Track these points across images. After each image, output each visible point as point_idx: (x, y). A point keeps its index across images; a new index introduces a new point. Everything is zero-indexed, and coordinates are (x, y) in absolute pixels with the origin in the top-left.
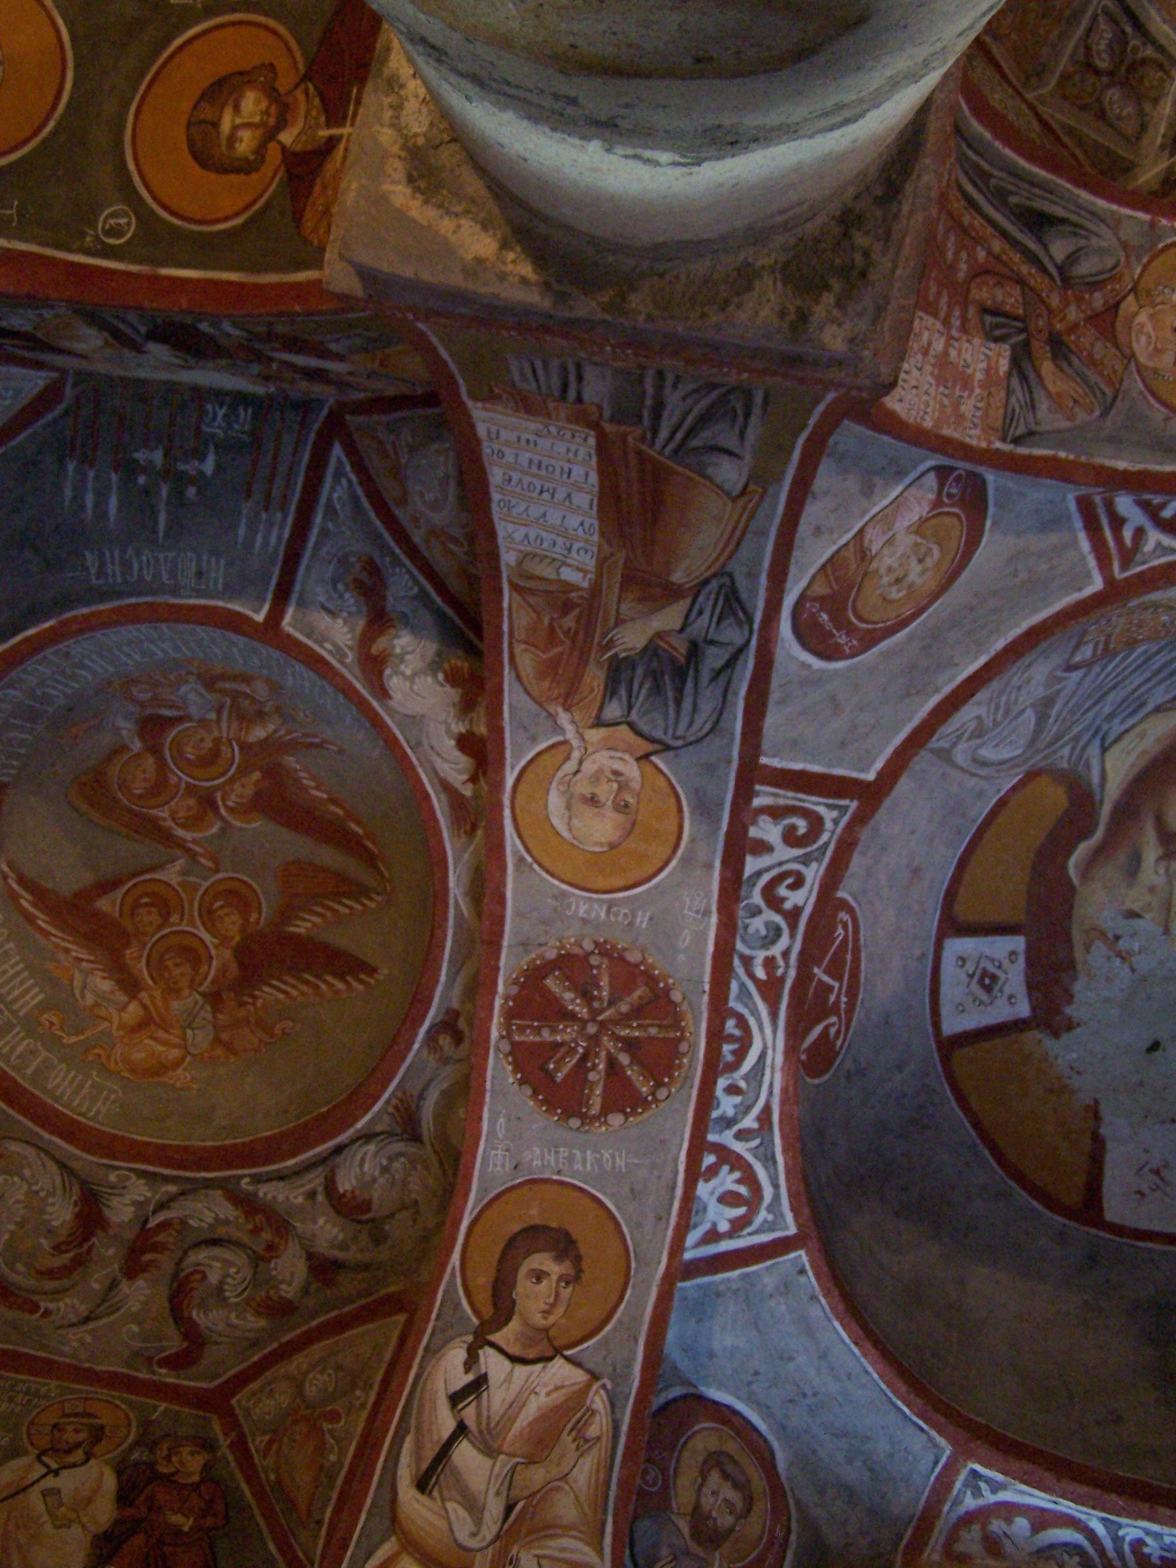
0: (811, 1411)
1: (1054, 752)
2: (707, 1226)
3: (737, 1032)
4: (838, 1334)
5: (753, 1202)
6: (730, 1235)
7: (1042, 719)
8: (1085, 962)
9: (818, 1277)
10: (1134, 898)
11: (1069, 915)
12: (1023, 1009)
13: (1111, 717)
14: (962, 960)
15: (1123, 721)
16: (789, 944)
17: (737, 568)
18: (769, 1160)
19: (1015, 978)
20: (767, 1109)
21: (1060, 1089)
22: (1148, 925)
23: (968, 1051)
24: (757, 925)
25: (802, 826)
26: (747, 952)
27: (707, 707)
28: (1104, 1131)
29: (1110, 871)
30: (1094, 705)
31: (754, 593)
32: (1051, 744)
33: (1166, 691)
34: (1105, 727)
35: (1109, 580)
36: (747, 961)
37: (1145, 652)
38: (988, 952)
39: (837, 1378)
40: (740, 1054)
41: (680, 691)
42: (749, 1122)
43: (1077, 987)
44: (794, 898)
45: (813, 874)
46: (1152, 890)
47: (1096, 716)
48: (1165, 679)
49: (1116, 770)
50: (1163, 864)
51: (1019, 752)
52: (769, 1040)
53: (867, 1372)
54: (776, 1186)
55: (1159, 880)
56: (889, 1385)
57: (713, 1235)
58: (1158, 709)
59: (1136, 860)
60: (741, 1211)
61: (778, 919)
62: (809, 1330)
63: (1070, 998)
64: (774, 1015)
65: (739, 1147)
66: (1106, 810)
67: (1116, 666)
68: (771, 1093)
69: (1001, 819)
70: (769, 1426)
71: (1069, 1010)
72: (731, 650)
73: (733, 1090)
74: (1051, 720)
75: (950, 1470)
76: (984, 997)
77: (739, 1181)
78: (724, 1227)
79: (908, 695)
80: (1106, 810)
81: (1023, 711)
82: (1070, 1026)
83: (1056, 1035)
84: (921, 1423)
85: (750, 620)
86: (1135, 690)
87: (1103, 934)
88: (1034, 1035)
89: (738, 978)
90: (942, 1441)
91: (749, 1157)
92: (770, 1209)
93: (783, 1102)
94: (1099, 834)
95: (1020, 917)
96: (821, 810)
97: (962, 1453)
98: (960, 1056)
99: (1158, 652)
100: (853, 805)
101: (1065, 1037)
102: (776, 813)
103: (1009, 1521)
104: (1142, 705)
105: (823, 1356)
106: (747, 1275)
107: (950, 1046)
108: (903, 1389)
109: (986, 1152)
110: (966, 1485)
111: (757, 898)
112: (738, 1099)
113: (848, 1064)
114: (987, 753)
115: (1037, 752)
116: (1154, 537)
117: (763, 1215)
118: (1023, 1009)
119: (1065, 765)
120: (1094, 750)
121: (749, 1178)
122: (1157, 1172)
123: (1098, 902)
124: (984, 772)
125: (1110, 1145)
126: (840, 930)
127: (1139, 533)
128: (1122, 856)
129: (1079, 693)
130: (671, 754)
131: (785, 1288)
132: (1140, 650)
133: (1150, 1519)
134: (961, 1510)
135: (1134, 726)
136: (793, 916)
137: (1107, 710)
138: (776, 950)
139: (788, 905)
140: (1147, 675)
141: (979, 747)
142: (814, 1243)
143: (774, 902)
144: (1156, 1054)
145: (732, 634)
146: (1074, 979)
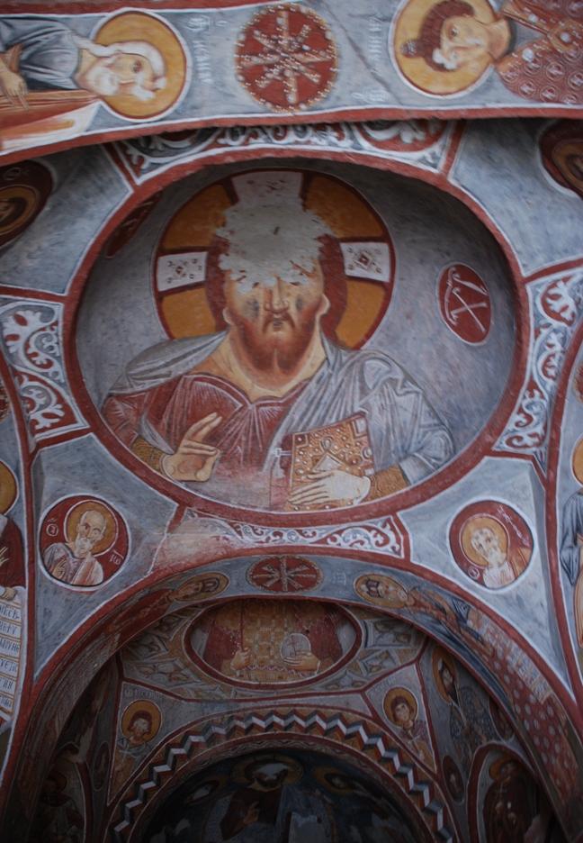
0: (521, 188)
1: (350, 359)
2: (569, 284)
3: (548, 369)
4: (507, 234)
5: (546, 295)
6: (558, 280)
7: (362, 380)
8: (314, 263)
9: (517, 264)
10: (295, 291)
11: (326, 282)
12: (344, 247)
13: (330, 376)
14: (378, 271)
15: (323, 373)
16: (523, 400)
17: (571, 589)
18: (537, 315)
19: (349, 259)
20: (536, 337)
21: (324, 215)
22: (289, 280)
23: (375, 235)
24: (536, 409)
25: (515, 442)
26: (542, 400)
27: (568, 516)
28: (300, 200)
29: (310, 301)
30: (340, 386)
31: (564, 579)
32: (352, 364)
33: (310, 391)
34: (330, 371)
35: (394, 515)
36: (542, 397)
37: (331, 418)
38: (366, 272)
39: (509, 212)
40: (548, 360)
41: (578, 520)
42: (544, 332)
43: (316, 254)
44: (520, 418)
45: (510, 426)
46: (289, 295)
47: (336, 378)
48: (315, 397)
49: (318, 349)
50: (287, 306)
51: (367, 363)
52: (533, 365)
53: (492, 215)
54: (535, 305)
55: (287, 299)
56: (481, 210)
57: (565, 280)
58: (310, 379)
59: (299, 307)
60: (552, 292)
61: (527, 411)
62: (523, 236)
63: (321, 250)
64: (532, 377)
65: (550, 320)
66: (317, 327)
67: (340, 410)
68: (534, 344)
69: (366, 328)
70: (542, 176)
71: (320, 245)
72: (564, 547)
73: (551, 346)
74: (357, 378)
75: (448, 167)
76: (365, 254)
77: (550, 305)
78: (561, 284)
79: (472, 483)
80: (317, 327)
81: (374, 386)
82: (319, 239)
83: (327, 236)
84: (463, 190)
85: (562, 565)
86: (324, 392)
87: (308, 275)
88: (337, 236)
89: (547, 391)
90: (452, 181)
91: (545, 315)
92: (538, 293)
93: (528, 340)
94: (318, 317)
95: (349, 284)
96: (506, 446)
97: (442, 178)
98: (379, 234)
99: (325, 416)
100: (494, 448)
101: (321, 234)
102: (526, 446)
103: (415, 140)
104: (318, 382)
105: (515, 223)
106: (552, 260)
107: (384, 238)
108: (475, 210)
109: (365, 197)
110: (438, 159)
111: (535, 418)
112: (551, 342)
113: (448, 259)
114: (386, 368)
115: (358, 361)
116: (379, 526)
117: (541, 291)
118: (344, 247)
119: (343, 351)
120: (331, 359)
121: (546, 306)
122: (273, 189)
123: (312, 288)
124: (382, 356)
125: (297, 195)
126: (454, 317)
127: (384, 526)
128: (305, 307)
129: (351, 394)
130: (578, 490)
131: (532, 257)
132: (333, 420)
133: (335, 153)
134: (441, 142)
135: (317, 371)
136: (521, 411)
137: (333, 380)
138: (528, 400)
139: (522, 415)
140: (323, 401)
141: (389, 372)
142: (518, 280)
143: (529, 418)
144: (273, 228)
145: (565, 554)
146: (319, 257)
